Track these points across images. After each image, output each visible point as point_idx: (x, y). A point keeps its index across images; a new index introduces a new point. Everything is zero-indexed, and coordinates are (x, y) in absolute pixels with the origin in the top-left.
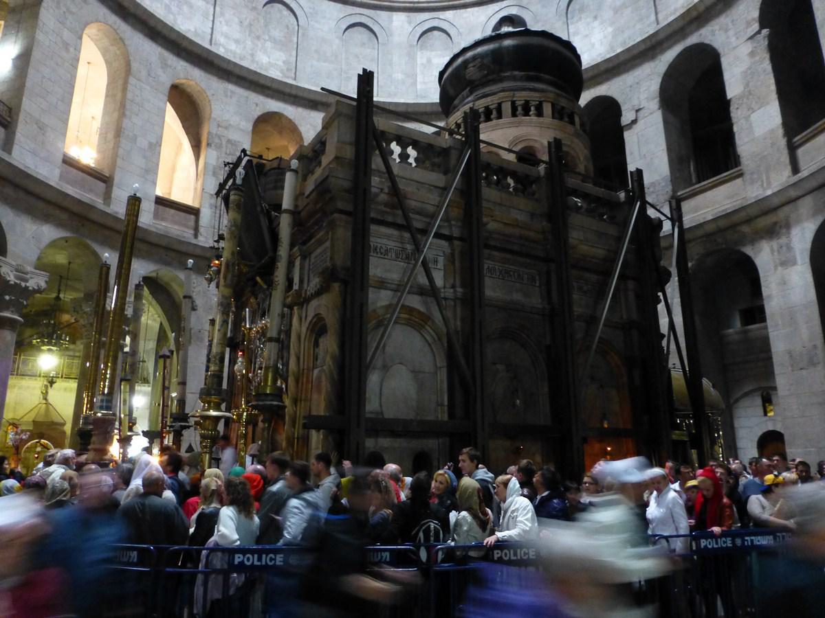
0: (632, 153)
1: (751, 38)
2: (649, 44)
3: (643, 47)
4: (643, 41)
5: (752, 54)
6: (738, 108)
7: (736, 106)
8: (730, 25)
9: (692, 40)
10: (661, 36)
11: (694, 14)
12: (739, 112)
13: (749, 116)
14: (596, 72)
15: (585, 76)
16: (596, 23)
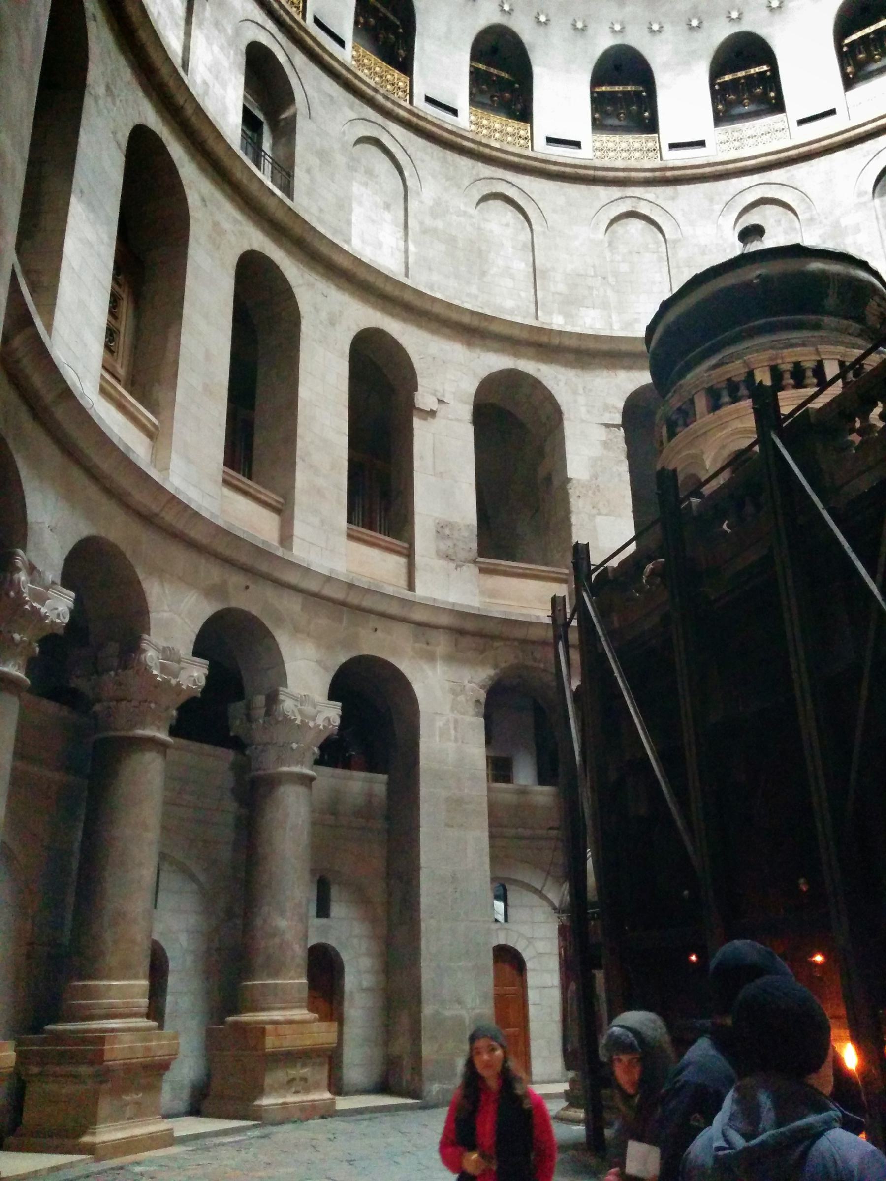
0: (422, 458)
1: (608, 426)
2: (475, 322)
3: (466, 319)
4: (473, 313)
5: (606, 445)
6: (579, 497)
7: (578, 494)
8: (581, 391)
9: (528, 366)
10: (494, 328)
11: (545, 339)
12: (581, 503)
13: (594, 516)
14: (397, 293)
15: (647, 364)
16: (388, 216)
